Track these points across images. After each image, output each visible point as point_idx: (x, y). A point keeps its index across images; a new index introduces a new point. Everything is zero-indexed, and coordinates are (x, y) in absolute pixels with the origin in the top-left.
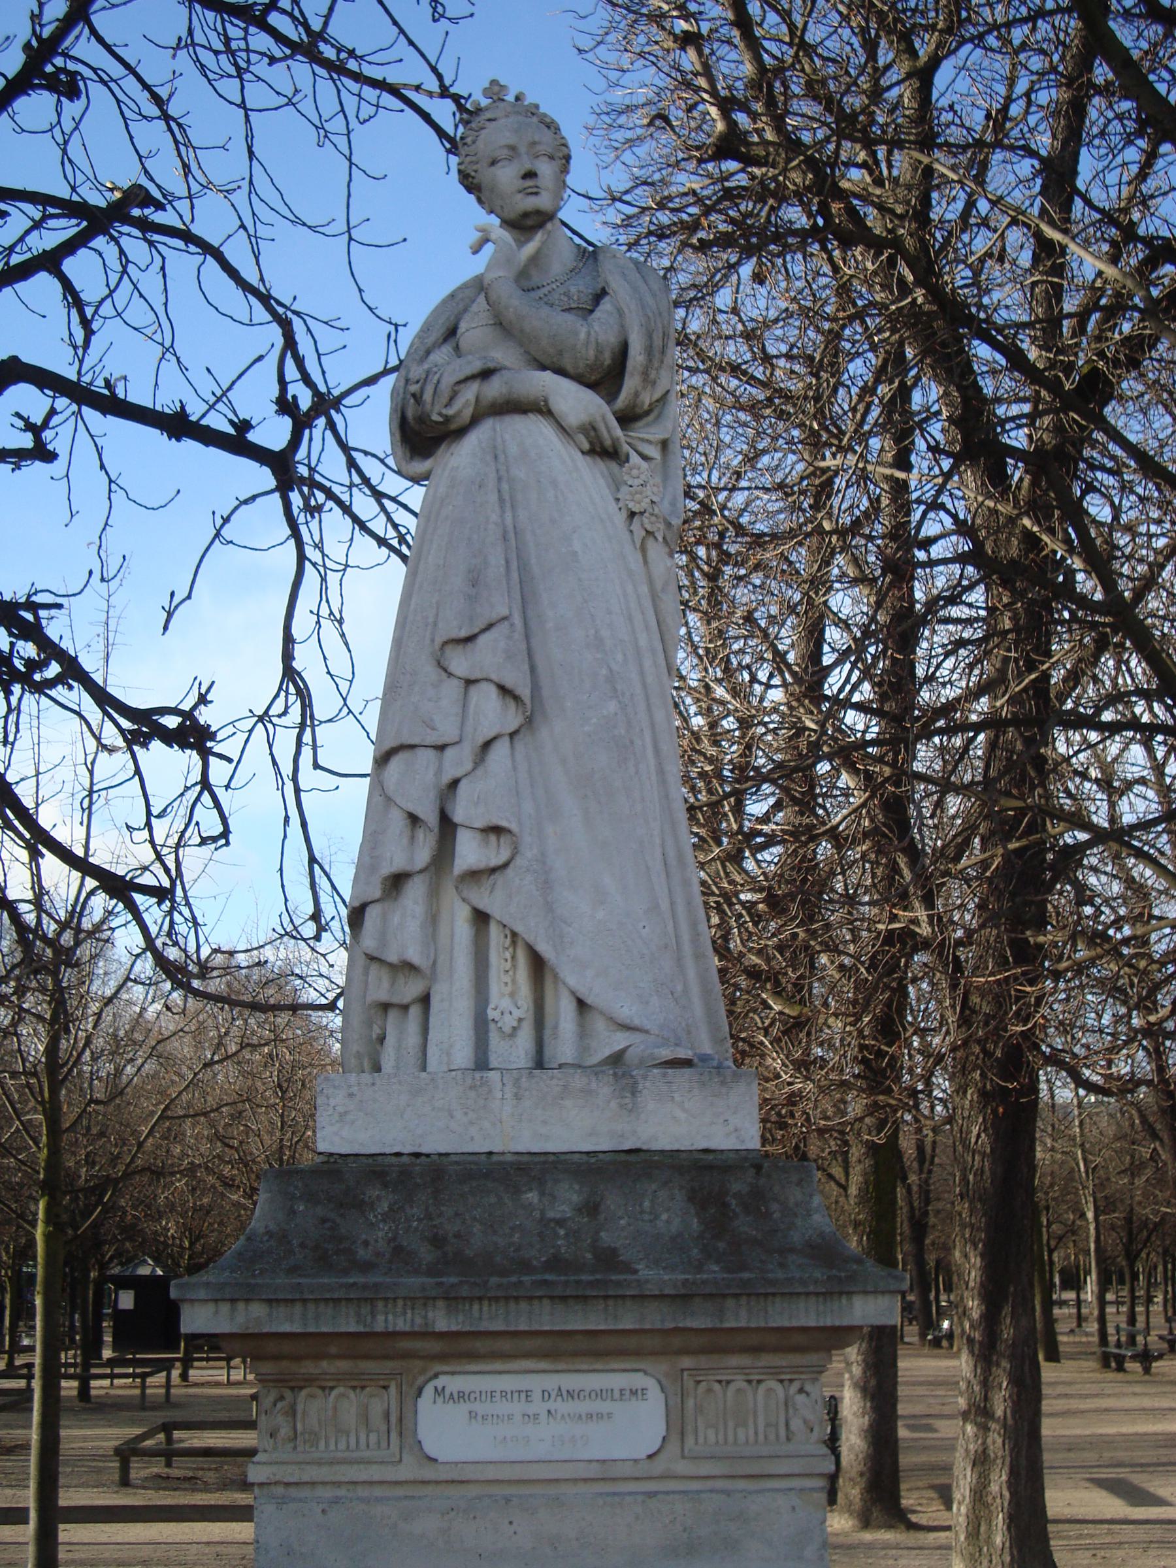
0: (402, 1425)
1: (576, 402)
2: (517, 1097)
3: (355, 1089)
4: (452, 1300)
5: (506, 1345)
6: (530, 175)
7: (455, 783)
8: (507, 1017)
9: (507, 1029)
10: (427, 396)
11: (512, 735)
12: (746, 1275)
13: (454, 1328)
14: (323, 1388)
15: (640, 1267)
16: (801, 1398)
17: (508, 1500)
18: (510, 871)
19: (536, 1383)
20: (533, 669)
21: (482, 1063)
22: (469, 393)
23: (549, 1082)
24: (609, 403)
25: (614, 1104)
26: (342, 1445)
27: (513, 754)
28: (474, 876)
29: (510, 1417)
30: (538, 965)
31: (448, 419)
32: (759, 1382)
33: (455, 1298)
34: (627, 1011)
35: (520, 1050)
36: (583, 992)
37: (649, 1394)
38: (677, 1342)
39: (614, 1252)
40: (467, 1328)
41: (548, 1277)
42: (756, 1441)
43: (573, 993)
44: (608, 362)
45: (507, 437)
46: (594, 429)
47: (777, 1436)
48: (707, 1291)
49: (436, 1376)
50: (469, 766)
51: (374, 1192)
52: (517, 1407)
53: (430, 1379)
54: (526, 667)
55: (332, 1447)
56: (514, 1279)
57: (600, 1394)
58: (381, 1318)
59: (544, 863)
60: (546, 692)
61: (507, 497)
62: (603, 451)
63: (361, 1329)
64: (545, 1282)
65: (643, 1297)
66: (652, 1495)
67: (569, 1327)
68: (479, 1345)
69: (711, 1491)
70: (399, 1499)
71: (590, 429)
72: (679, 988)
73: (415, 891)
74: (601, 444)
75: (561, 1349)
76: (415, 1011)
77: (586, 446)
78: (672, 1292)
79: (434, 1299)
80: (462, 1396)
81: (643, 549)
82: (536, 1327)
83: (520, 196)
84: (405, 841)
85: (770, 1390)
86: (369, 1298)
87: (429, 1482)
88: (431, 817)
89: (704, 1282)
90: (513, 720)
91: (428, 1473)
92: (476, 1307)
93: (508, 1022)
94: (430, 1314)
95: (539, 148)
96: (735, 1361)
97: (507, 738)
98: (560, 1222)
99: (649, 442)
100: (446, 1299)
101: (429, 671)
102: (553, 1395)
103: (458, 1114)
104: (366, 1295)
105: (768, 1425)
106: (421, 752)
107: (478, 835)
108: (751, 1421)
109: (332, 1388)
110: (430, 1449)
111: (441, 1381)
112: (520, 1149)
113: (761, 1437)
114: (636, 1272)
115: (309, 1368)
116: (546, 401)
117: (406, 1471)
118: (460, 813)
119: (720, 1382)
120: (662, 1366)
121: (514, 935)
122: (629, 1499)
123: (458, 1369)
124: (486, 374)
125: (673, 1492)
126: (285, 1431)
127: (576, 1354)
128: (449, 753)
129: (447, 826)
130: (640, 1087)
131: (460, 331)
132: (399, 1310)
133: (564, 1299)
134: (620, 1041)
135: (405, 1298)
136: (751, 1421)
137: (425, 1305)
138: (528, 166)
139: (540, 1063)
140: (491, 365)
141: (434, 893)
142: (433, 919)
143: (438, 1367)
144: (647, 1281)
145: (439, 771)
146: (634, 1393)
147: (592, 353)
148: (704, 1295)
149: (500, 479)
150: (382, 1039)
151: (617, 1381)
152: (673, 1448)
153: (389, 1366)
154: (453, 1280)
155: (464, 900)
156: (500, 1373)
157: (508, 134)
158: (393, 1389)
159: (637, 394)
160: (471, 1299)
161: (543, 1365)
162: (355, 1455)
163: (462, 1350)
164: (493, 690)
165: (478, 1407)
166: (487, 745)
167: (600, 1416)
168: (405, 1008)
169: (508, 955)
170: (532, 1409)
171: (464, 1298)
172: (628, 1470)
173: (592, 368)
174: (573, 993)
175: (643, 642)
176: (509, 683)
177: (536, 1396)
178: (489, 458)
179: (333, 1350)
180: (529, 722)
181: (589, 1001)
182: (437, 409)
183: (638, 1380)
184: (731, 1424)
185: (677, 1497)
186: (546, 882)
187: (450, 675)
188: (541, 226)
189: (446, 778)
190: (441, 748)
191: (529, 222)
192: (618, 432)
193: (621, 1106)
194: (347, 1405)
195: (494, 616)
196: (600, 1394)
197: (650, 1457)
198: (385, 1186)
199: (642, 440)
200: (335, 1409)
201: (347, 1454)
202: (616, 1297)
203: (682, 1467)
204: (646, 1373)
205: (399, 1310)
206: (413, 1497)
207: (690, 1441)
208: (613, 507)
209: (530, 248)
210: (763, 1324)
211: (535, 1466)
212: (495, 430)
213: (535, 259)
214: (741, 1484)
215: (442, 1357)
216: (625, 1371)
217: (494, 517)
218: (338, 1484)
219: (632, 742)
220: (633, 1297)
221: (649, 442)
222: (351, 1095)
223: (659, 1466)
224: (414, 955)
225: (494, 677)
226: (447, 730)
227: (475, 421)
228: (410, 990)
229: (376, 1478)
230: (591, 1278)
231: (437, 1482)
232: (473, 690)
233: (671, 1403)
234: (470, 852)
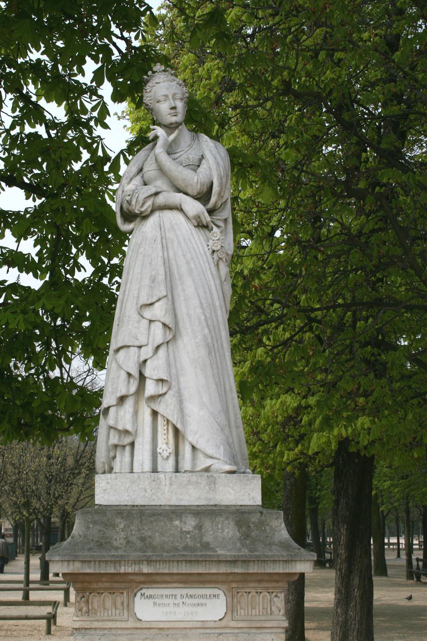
0: (129, 607)
1: (194, 207)
2: (171, 484)
3: (109, 481)
4: (149, 562)
5: (167, 578)
6: (174, 108)
7: (145, 361)
8: (165, 452)
9: (165, 457)
10: (134, 202)
11: (167, 343)
12: (257, 553)
13: (150, 572)
14: (99, 593)
15: (218, 550)
16: (276, 599)
18: (167, 396)
19: (178, 592)
20: (175, 315)
21: (155, 470)
22: (149, 203)
23: (183, 478)
24: (204, 205)
25: (207, 487)
28: (153, 398)
30: (177, 431)
31: (141, 213)
32: (261, 592)
33: (151, 561)
34: (210, 452)
35: (170, 465)
36: (194, 443)
38: (231, 578)
39: (208, 544)
40: (155, 572)
41: (184, 553)
42: (259, 615)
43: (190, 443)
44: (205, 190)
45: (164, 220)
46: (199, 217)
47: (267, 612)
48: (243, 559)
49: (141, 589)
50: (151, 354)
51: (118, 520)
52: (171, 601)
53: (139, 590)
55: (102, 615)
56: (172, 554)
57: (202, 596)
58: (123, 568)
59: (180, 393)
60: (181, 325)
62: (202, 226)
63: (116, 572)
64: (184, 555)
65: (219, 561)
67: (192, 572)
68: (158, 578)
69: (243, 633)
71: (198, 218)
72: (231, 441)
73: (129, 404)
74: (202, 223)
75: (187, 580)
76: (128, 449)
77: (196, 224)
78: (230, 559)
79: (143, 561)
80: (151, 597)
81: (217, 265)
82: (180, 572)
83: (169, 116)
84: (126, 383)
85: (264, 596)
86: (117, 561)
87: (139, 628)
88: (135, 373)
89: (242, 556)
90: (169, 336)
91: (139, 625)
92: (158, 564)
93: (165, 454)
94: (141, 567)
95: (177, 96)
96: (252, 585)
97: (166, 344)
98: (188, 532)
99: (220, 220)
100: (147, 561)
101: (135, 316)
102: (185, 596)
103: (148, 491)
104: (118, 559)
105: (263, 608)
106: (132, 348)
107: (154, 382)
108: (257, 607)
109: (102, 593)
110: (139, 616)
111: (143, 591)
112: (172, 503)
113: (261, 613)
114: (217, 552)
115: (94, 586)
116: (180, 206)
117: (130, 624)
118: (147, 373)
119: (246, 592)
120: (225, 587)
121: (168, 420)
122: (212, 635)
123: (149, 586)
124: (157, 194)
125: (229, 633)
126: (84, 609)
127: (192, 582)
128: (143, 348)
129: (142, 378)
130: (217, 481)
131: (144, 171)
132: (130, 565)
133: (190, 561)
134: (208, 462)
135: (132, 560)
136: (257, 607)
137: (139, 563)
138: (173, 105)
139: (177, 471)
140: (159, 190)
141: (137, 403)
142: (136, 413)
144: (221, 555)
145: (139, 356)
146: (214, 596)
147: (199, 187)
148: (242, 561)
149: (162, 238)
150: (114, 458)
152: (229, 616)
153: (123, 585)
154: (150, 554)
155: (148, 406)
156: (165, 588)
157: (164, 90)
158: (125, 594)
159: (216, 203)
160: (156, 561)
161: (181, 585)
162: (111, 618)
163: (152, 580)
164: (161, 325)
165: (158, 601)
166: (158, 347)
167: (202, 605)
168: (124, 447)
169: (165, 428)
170: (176, 602)
171: (154, 561)
172: (212, 625)
173: (199, 193)
174: (190, 443)
175: (217, 304)
176: (167, 323)
177: (179, 597)
178: (158, 229)
179: (104, 579)
180: (174, 336)
181: (197, 447)
182: (137, 208)
183: (216, 591)
184: (250, 608)
185: (229, 635)
187: (143, 318)
188: (177, 127)
189: (142, 359)
190: (140, 347)
191: (173, 126)
192: (209, 219)
193: (210, 488)
194: (108, 600)
195: (161, 295)
197: (220, 620)
198: (122, 518)
199: (218, 219)
200: (104, 601)
201: (108, 618)
202: (209, 561)
203: (233, 624)
204: (219, 589)
205: (130, 565)
206: (132, 634)
208: (206, 248)
209: (172, 137)
210: (263, 572)
211: (178, 623)
212: (160, 216)
213: (174, 141)
214: (254, 631)
215: (144, 583)
216: (211, 588)
217: (161, 254)
218: (105, 629)
220: (216, 561)
221: (220, 220)
222: (108, 483)
223: (223, 623)
224: (129, 427)
225: (162, 320)
226: (142, 340)
227: (153, 211)
228: (127, 440)
229: (119, 627)
230: (200, 554)
231: (142, 628)
232: (153, 325)
233: (228, 600)
234: (151, 388)
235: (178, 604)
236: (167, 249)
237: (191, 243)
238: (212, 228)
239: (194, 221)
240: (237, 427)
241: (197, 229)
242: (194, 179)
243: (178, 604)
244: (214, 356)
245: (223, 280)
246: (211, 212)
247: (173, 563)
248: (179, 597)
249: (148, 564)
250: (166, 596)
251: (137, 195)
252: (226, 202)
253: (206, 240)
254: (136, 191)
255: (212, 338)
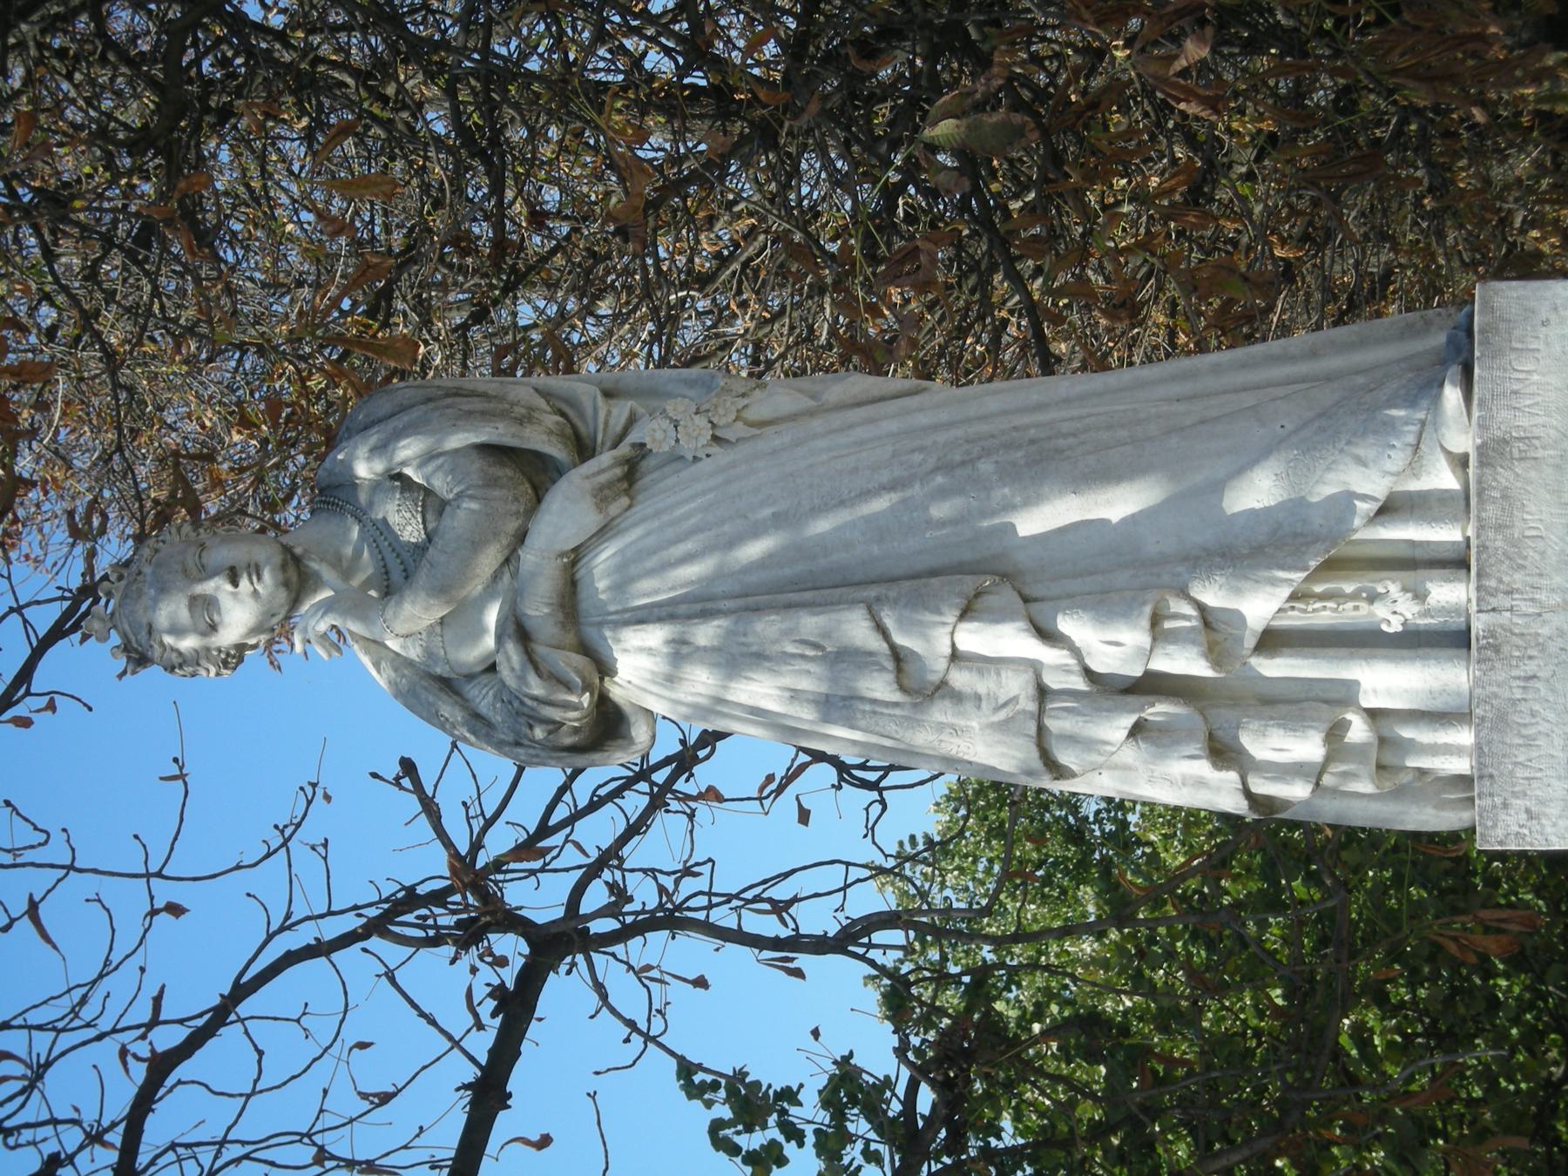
1: (566, 514)
3: (1498, 800)
11: (1026, 600)
20: (934, 573)
27: (1052, 599)
46: (601, 488)
54: (934, 581)
59: (1197, 558)
61: (698, 607)
71: (603, 496)
74: (620, 480)
77: (625, 501)
97: (1035, 607)
116: (562, 555)
130: (1499, 433)
168: (1383, 741)
175: (892, 426)
180: (1007, 576)
186: (1223, 555)
188: (297, 560)
192: (605, 458)
208: (705, 466)
219: (1032, 442)
236: (709, 600)
237: (687, 516)
238: (634, 445)
239: (614, 509)
240: (1313, 354)
241: (640, 498)
242: (473, 511)
244: (1071, 440)
245: (812, 403)
246: (584, 449)
251: (529, 702)
252: (545, 394)
253: (674, 466)
254: (516, 704)
255: (1010, 446)
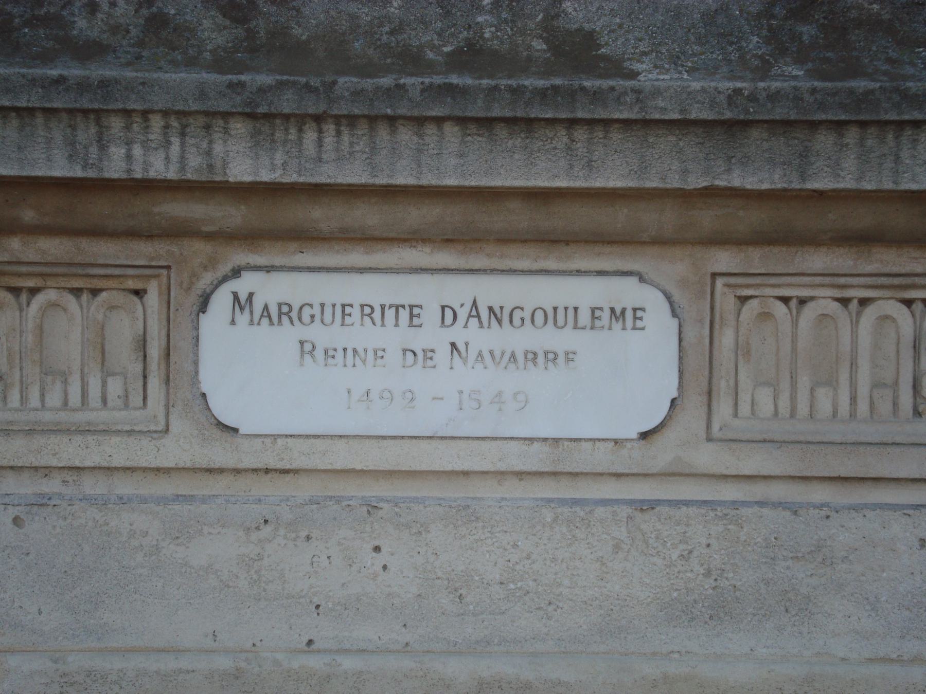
0: (171, 364)
4: (262, 119)
5: (367, 215)
12: (861, 85)
13: (266, 176)
14: (15, 291)
15: (637, 67)
17: (372, 508)
19: (428, 292)
26: (54, 399)
29: (379, 354)
32: (864, 302)
33: (269, 117)
37: (649, 319)
38: (707, 218)
39: (589, 39)
40: (292, 177)
41: (454, 79)
42: (853, 415)
47: (895, 404)
48: (779, 113)
49: (236, 273)
52: (391, 336)
53: (225, 279)
55: (35, 402)
56: (387, 81)
57: (552, 317)
58: (117, 152)
63: (79, 173)
64: (450, 89)
65: (647, 123)
66: (646, 506)
67: (497, 182)
68: (318, 214)
69: (762, 504)
70: (163, 501)
75: (475, 225)
78: (705, 115)
79: (226, 115)
80: (285, 313)
82: (429, 179)
85: (886, 317)
86: (93, 111)
87: (221, 471)
89: (774, 97)
91: (219, 454)
92: (310, 136)
94: (218, 148)
96: (818, 260)
100: (251, 116)
102: (463, 314)
104: (85, 103)
105: (877, 385)
108: (844, 377)
109: (34, 291)
110: (224, 407)
111: (245, 284)
113: (863, 407)
114: (634, 75)
117: (171, 452)
119: (785, 300)
120: (674, 267)
122: (600, 511)
123: (278, 261)
125: (687, 503)
127: (506, 239)
132: (156, 133)
133: (487, 123)
135: (166, 113)
136: (844, 377)
137: (207, 127)
143: (241, 257)
144: (657, 92)
146: (617, 315)
148: (771, 124)
151: (585, 292)
152: (692, 419)
153: (143, 251)
154: (265, 79)
156: (362, 270)
158: (153, 298)
160: (301, 120)
162: (80, 417)
163: (285, 219)
165: (319, 334)
167: (551, 357)
170: (420, 340)
171: (287, 117)
172: (602, 459)
177: (431, 315)
183: (628, 292)
184: (804, 381)
185: (692, 511)
194: (68, 324)
196: (552, 317)
197: (644, 435)
200: (40, 330)
201: (63, 416)
202: (591, 123)
203: (707, 457)
204: (642, 279)
205: (156, 133)
207: (723, 409)
210: (888, 185)
211: (424, 445)
214: (820, 494)
215: (250, 237)
216: (601, 273)
218: (46, 471)
220: (627, 124)
223: (661, 455)
229: (118, 461)
230: (541, 83)
231: (237, 471)
233: (690, 335)
235: (429, 353)
243: (429, 353)
247: (393, 131)
248: (431, 315)
249: (255, 134)
250: (367, 311)
